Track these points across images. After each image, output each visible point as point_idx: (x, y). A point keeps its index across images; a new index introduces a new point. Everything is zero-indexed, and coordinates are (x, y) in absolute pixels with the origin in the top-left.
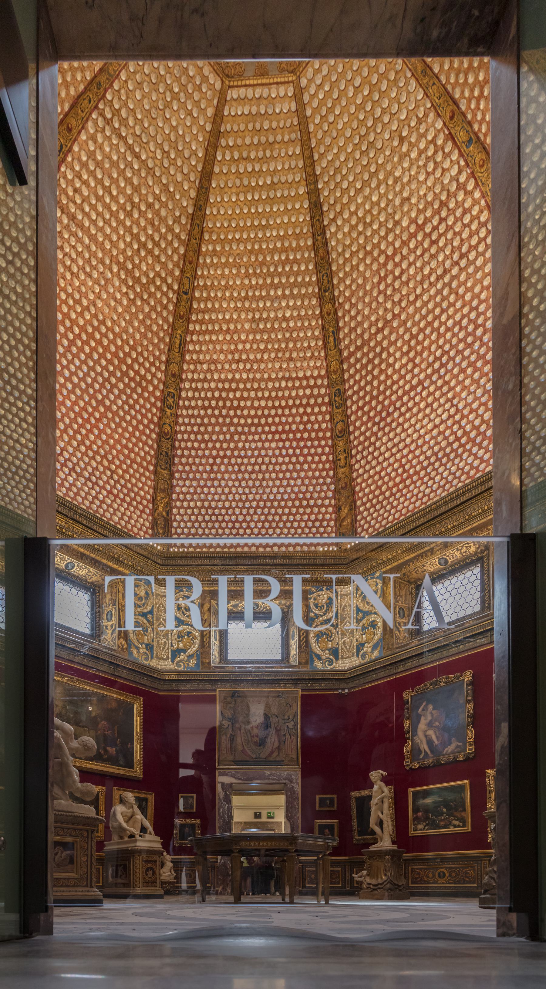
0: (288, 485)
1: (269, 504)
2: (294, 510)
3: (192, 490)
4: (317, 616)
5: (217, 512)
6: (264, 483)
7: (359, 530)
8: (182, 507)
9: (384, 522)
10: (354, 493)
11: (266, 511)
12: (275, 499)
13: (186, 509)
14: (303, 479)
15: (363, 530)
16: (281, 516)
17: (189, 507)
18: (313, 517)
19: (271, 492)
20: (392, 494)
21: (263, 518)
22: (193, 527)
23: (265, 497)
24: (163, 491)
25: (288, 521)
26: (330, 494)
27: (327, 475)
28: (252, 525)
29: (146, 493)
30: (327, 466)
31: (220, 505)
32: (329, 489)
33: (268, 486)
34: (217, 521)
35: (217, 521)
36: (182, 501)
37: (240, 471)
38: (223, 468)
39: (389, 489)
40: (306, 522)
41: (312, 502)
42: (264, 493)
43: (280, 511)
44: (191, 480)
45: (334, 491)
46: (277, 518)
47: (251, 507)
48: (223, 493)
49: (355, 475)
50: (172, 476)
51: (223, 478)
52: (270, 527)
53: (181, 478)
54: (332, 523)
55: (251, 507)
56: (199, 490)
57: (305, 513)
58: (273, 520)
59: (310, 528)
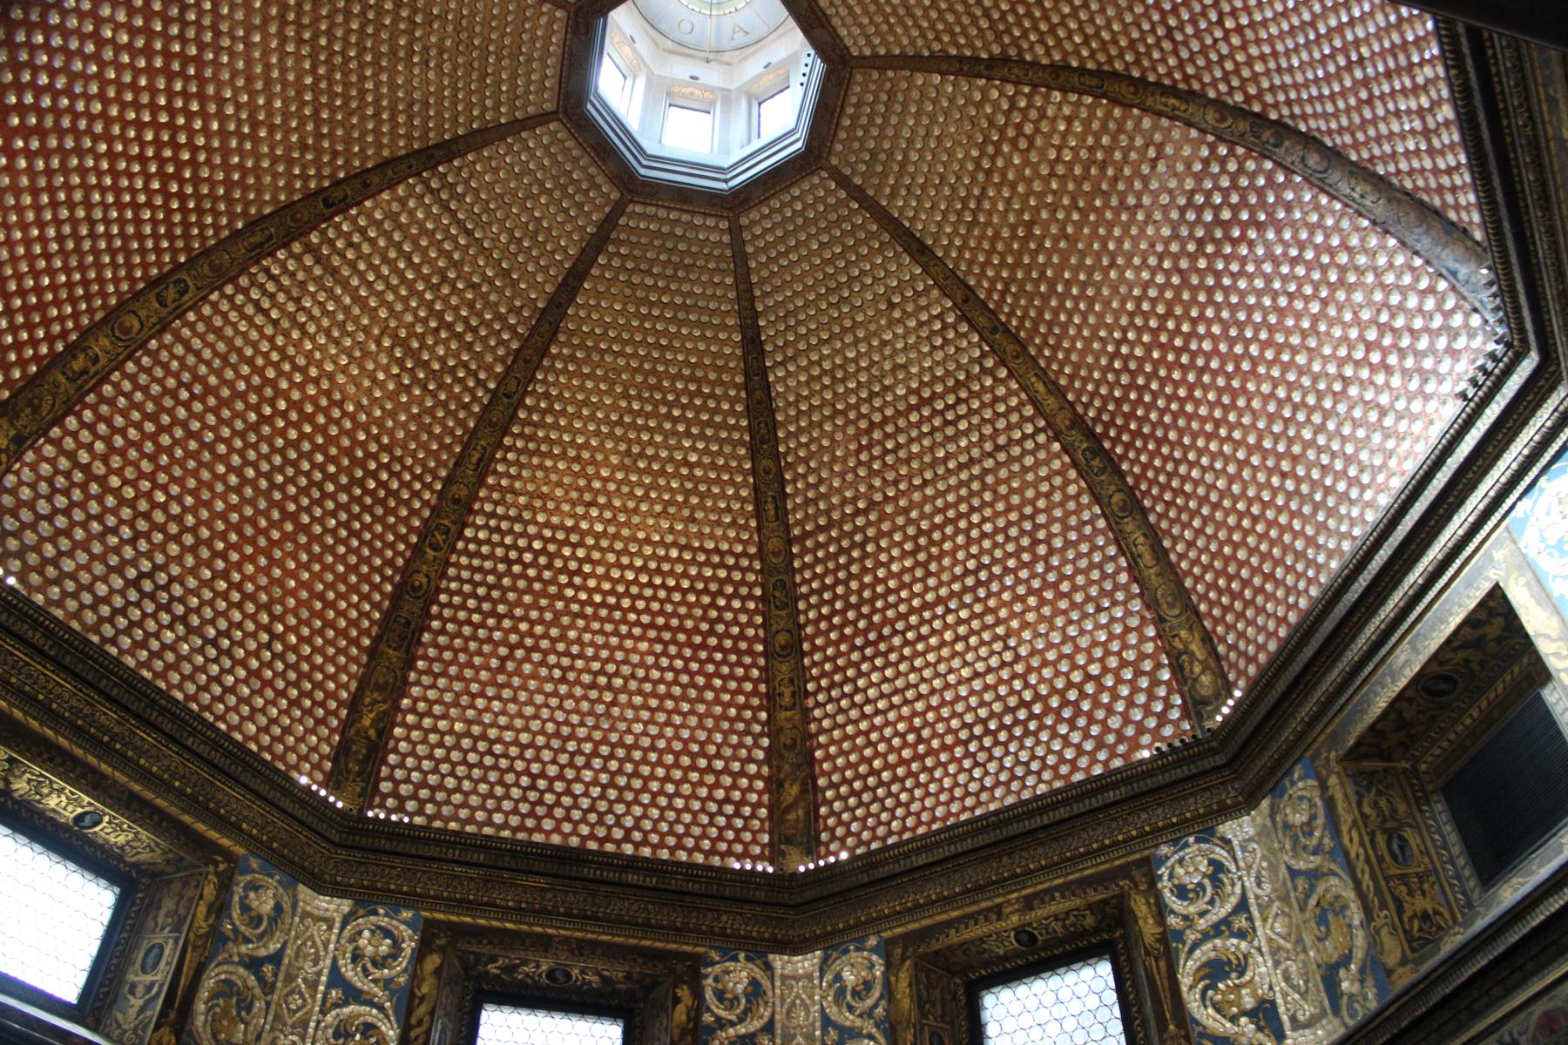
0: (668, 723)
1: (621, 752)
2: (677, 774)
4: (721, 1024)
5: (498, 748)
6: (616, 711)
7: (824, 836)
8: (418, 726)
9: (881, 831)
10: (812, 761)
11: (614, 765)
12: (636, 746)
13: (427, 732)
14: (701, 717)
15: (833, 838)
16: (646, 780)
17: (435, 730)
18: (720, 794)
20: (895, 779)
21: (604, 778)
22: (435, 771)
23: (614, 737)
24: (381, 688)
25: (662, 792)
26: (760, 755)
27: (755, 719)
28: (578, 789)
29: (339, 686)
30: (755, 701)
32: (757, 745)
33: (623, 718)
34: (495, 767)
35: (495, 767)
36: (422, 716)
37: (563, 680)
38: (527, 668)
39: (887, 766)
40: (703, 801)
41: (719, 764)
42: (613, 729)
43: (645, 770)
44: (451, 679)
45: (768, 751)
46: (637, 784)
48: (520, 715)
49: (813, 727)
50: (411, 665)
51: (524, 687)
52: (620, 800)
53: (429, 672)
54: (763, 812)
55: (580, 752)
56: (465, 700)
57: (701, 783)
58: (628, 787)
59: (712, 816)
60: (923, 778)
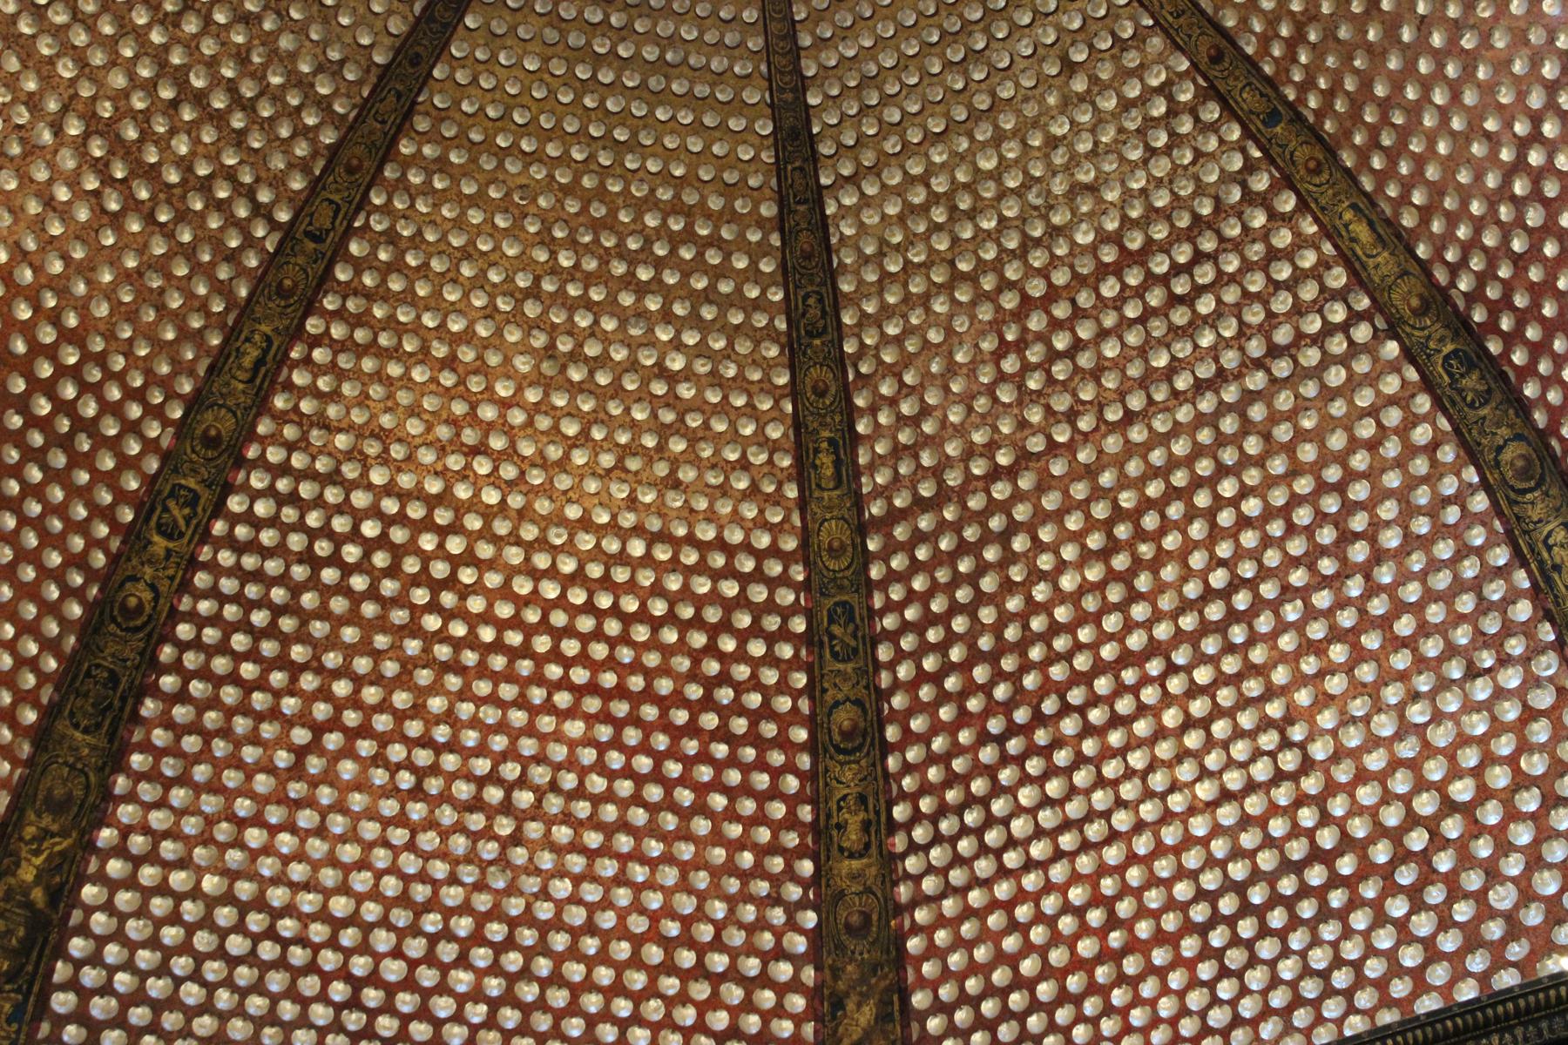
0: (621, 880)
1: (528, 936)
2: (637, 980)
3: (191, 825)
5: (287, 927)
6: (519, 855)
8: (131, 883)
10: (901, 957)
11: (513, 961)
12: (557, 924)
13: (147, 893)
14: (685, 868)
16: (576, 990)
17: (163, 889)
19: (544, 894)
20: (1063, 997)
21: (494, 986)
22: (162, 970)
23: (515, 907)
24: (57, 807)
26: (799, 944)
27: (790, 874)
30: (791, 839)
31: (308, 902)
32: (792, 925)
33: (532, 869)
34: (281, 963)
35: (281, 963)
36: (137, 862)
37: (417, 793)
38: (347, 769)
39: (1047, 971)
41: (719, 962)
42: (512, 890)
45: (815, 937)
46: (559, 998)
47: (447, 934)
48: (332, 861)
49: (904, 892)
50: (118, 762)
51: (340, 807)
53: (153, 775)
55: (447, 934)
56: (223, 831)
57: (683, 998)
58: (541, 1004)
60: (1118, 997)
